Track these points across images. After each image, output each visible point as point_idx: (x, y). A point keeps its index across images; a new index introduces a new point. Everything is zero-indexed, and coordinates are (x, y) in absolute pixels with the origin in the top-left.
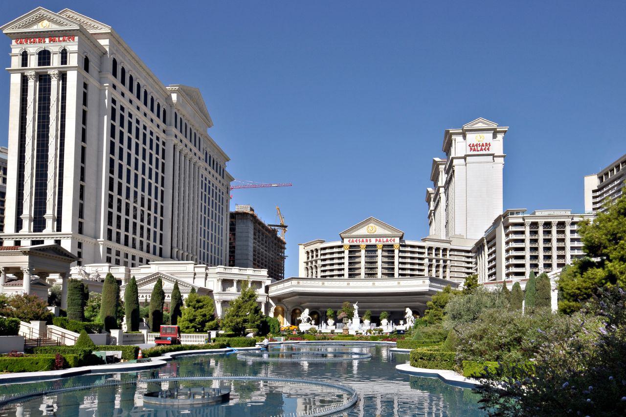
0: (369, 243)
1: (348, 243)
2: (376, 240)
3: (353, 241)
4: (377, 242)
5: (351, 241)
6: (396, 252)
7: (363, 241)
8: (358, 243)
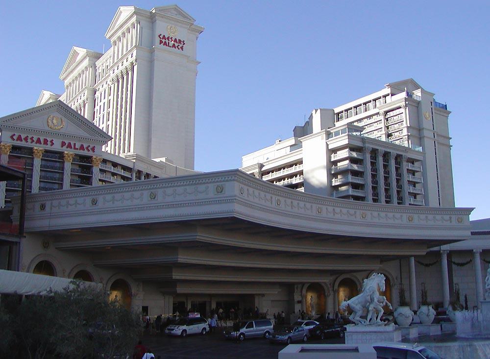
0: (49, 147)
1: (10, 140)
2: (63, 144)
3: (19, 138)
4: (65, 147)
5: (15, 137)
6: (96, 170)
7: (39, 141)
8: (29, 144)
